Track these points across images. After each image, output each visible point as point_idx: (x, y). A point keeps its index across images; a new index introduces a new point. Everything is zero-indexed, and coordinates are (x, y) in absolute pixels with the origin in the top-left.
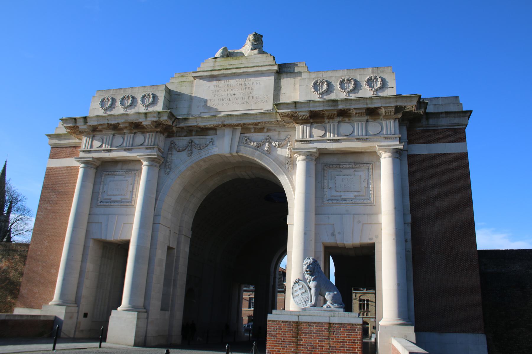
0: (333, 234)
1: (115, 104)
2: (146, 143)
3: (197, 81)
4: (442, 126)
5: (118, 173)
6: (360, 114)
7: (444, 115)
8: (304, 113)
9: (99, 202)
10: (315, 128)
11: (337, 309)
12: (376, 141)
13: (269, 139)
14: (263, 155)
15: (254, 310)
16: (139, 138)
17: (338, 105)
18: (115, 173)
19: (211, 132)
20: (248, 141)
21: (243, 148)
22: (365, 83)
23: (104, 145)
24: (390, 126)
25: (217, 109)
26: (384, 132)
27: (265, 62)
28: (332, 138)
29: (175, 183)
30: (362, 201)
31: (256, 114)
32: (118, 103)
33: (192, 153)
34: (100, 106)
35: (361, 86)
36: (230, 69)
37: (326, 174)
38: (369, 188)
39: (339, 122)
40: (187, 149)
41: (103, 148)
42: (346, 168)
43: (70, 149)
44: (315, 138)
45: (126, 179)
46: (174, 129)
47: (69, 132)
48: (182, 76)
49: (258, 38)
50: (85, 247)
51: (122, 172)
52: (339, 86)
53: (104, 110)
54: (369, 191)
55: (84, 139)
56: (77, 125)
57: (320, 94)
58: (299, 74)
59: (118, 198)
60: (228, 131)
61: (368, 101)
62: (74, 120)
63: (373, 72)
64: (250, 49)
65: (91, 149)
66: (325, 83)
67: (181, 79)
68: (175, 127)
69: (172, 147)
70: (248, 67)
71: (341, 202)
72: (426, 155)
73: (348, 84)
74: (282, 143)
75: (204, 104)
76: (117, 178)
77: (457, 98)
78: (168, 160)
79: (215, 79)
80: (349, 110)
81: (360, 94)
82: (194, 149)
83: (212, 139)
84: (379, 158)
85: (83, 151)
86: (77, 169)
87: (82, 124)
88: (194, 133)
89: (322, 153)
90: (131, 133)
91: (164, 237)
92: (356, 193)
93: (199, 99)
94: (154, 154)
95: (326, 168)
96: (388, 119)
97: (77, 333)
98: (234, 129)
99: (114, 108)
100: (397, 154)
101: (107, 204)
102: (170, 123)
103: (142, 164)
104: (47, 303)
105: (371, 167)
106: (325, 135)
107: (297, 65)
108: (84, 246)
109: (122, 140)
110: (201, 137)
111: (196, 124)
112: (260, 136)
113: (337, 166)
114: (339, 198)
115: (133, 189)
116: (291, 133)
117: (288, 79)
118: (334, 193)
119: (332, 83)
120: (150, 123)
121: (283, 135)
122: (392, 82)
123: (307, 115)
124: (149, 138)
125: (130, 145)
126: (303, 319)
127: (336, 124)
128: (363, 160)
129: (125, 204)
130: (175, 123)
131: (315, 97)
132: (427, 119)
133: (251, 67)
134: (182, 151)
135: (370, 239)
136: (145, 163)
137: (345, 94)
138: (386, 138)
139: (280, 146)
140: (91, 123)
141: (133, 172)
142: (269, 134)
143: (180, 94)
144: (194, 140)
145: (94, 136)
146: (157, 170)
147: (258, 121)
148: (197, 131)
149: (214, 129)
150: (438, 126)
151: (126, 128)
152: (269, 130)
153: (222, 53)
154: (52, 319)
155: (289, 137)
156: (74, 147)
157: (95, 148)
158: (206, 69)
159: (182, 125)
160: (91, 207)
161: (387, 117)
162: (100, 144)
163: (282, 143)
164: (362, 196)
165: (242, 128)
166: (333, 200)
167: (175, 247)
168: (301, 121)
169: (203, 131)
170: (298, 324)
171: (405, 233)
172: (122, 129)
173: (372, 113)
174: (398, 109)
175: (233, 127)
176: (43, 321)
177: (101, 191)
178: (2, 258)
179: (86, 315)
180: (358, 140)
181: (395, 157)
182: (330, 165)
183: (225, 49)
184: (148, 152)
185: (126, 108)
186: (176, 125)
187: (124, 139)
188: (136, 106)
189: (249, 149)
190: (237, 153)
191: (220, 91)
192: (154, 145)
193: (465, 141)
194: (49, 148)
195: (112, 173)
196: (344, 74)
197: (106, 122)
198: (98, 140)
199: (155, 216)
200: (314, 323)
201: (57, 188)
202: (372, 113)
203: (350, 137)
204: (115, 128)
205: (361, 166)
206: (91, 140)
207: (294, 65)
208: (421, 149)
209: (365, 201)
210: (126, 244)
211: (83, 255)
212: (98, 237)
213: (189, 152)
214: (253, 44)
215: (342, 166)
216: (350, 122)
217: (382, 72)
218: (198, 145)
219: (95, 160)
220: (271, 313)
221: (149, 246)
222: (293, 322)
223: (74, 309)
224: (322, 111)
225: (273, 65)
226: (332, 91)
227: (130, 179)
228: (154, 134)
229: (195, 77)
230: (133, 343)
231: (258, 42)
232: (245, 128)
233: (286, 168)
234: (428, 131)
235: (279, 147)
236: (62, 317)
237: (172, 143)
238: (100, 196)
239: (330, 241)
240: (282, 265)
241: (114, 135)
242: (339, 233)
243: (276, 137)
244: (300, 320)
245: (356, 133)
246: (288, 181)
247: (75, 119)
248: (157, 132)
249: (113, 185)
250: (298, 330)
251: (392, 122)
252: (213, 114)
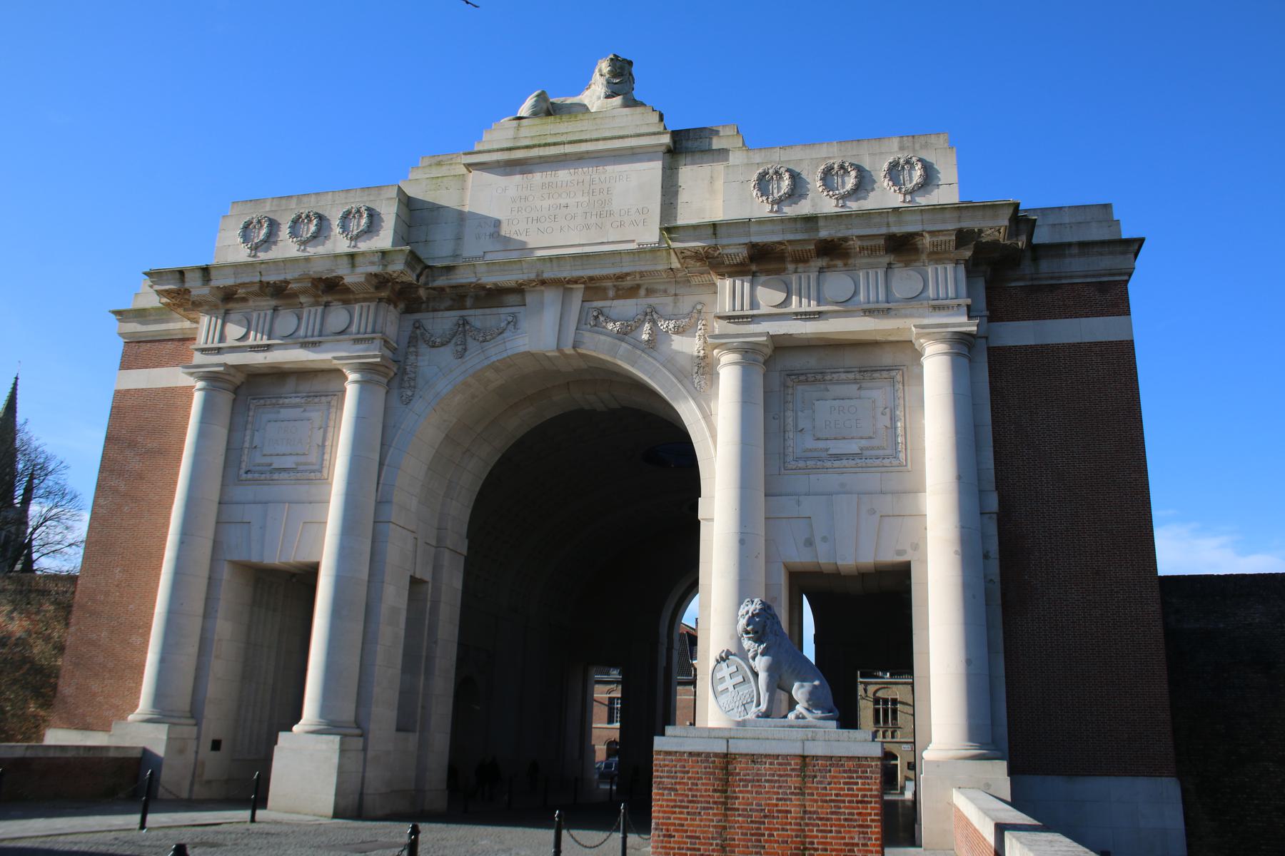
0: (809, 543)
1: (276, 235)
2: (354, 328)
3: (475, 173)
4: (1071, 277)
5: (287, 401)
6: (873, 251)
7: (1075, 251)
8: (734, 248)
9: (242, 471)
10: (764, 285)
11: (822, 723)
12: (911, 316)
13: (651, 315)
14: (639, 352)
15: (621, 728)
16: (338, 317)
17: (817, 230)
18: (281, 401)
19: (512, 298)
20: (602, 318)
21: (587, 337)
22: (883, 174)
23: (252, 333)
24: (946, 279)
25: (525, 243)
26: (931, 292)
27: (639, 125)
28: (805, 308)
29: (426, 423)
30: (878, 462)
31: (619, 253)
32: (284, 232)
33: (465, 350)
34: (240, 240)
35: (874, 182)
36: (555, 144)
37: (789, 398)
38: (896, 428)
39: (821, 270)
41: (250, 341)
42: (839, 382)
43: (170, 345)
44: (764, 309)
45: (307, 414)
46: (422, 292)
47: (167, 305)
48: (439, 164)
49: (622, 68)
50: (212, 582)
51: (298, 400)
52: (819, 183)
53: (251, 249)
54: (896, 436)
55: (205, 320)
56: (187, 285)
57: (773, 203)
58: (723, 153)
59: (289, 462)
60: (551, 297)
61: (892, 219)
62: (177, 275)
63: (902, 148)
64: (602, 95)
65: (221, 345)
66: (787, 176)
67: (436, 172)
68: (425, 288)
69: (417, 337)
70: (597, 140)
71: (828, 464)
72: (1031, 346)
73: (842, 176)
74: (684, 322)
75: (492, 230)
76: (285, 413)
77: (1107, 207)
79: (518, 168)
80: (845, 239)
81: (871, 202)
82: (469, 340)
83: (514, 315)
84: (918, 355)
85: (203, 350)
86: (187, 392)
87: (199, 283)
88: (469, 302)
89: (781, 346)
90: (317, 304)
91: (401, 555)
92: (864, 443)
93: (483, 220)
94: (373, 354)
95: (790, 383)
96: (938, 261)
97: (196, 787)
98: (566, 289)
99: (275, 243)
100: (963, 346)
101: (263, 476)
102: (411, 277)
103: (346, 378)
104: (125, 718)
105: (899, 378)
106: (786, 302)
107: (717, 132)
108: (210, 578)
109: (295, 321)
110: (488, 311)
111: (474, 280)
112: (628, 307)
113: (817, 378)
114: (824, 455)
115: (324, 440)
116: (705, 298)
117: (695, 167)
118: (810, 443)
119: (804, 175)
120: (362, 279)
121: (686, 303)
122: (948, 172)
123: (744, 253)
124: (361, 316)
125: (316, 333)
126: (738, 747)
127: (813, 276)
128: (881, 363)
129: (306, 475)
130: (423, 279)
131: (762, 209)
132: (1035, 260)
133: (605, 139)
134: (443, 345)
135: (899, 553)
136: (352, 376)
137: (834, 202)
138: (936, 308)
139: (679, 331)
140: (220, 281)
141: (324, 399)
142: (652, 301)
143: (436, 208)
145: (227, 312)
146: (381, 392)
147: (625, 270)
148: (477, 298)
149: (519, 289)
150: (1060, 278)
151: (304, 292)
152: (650, 292)
153: (535, 106)
154: (138, 754)
155: (699, 307)
156: (180, 340)
157: (230, 341)
158: (496, 146)
159: (441, 282)
160: (223, 485)
161: (937, 256)
162: (243, 331)
163: (684, 322)
164: (878, 448)
165: (587, 289)
166: (806, 459)
167: (427, 577)
168: (729, 270)
169: (492, 296)
170: (727, 758)
171: (984, 537)
172: (294, 295)
173: (901, 247)
174: (963, 237)
175: (564, 285)
176: (116, 759)
177: (247, 445)
178: (12, 612)
179: (216, 745)
180: (869, 312)
181: (958, 354)
182: (798, 375)
183: (542, 97)
184: (359, 350)
185: (304, 243)
186: (426, 283)
187: (299, 319)
188: (327, 238)
189: (603, 338)
190: (574, 348)
191: (531, 198)
192: (374, 332)
193: (1127, 312)
194: (120, 343)
196: (832, 153)
197: (257, 279)
198: (238, 323)
199: (379, 503)
200: (767, 756)
201: (140, 439)
202: (901, 247)
203: (847, 307)
204: (279, 292)
205: (876, 375)
206: (220, 322)
207: (710, 132)
208: (1020, 334)
209: (886, 462)
210: (311, 572)
211: (207, 599)
212: (242, 556)
213: (459, 348)
214: (608, 82)
215: (828, 377)
216: (848, 268)
217: (925, 146)
218: (479, 330)
219: (232, 371)
220: (663, 734)
221: (365, 576)
222: (716, 755)
223: (189, 731)
224: (780, 243)
225: (659, 133)
226: (803, 196)
227: (316, 416)
228: (373, 305)
229: (469, 166)
230: (331, 812)
231: (622, 79)
232: (593, 288)
233: (693, 383)
234: (1039, 289)
235: (677, 333)
236: (159, 750)
237: (417, 326)
238: (245, 458)
239: (801, 557)
240: (688, 619)
241: (275, 309)
242: (824, 539)
243: (670, 310)
244: (732, 750)
245: (862, 297)
246: (700, 416)
247: (181, 273)
248: (380, 300)
249: (276, 432)
250: (728, 774)
251: (950, 267)
252: (514, 256)
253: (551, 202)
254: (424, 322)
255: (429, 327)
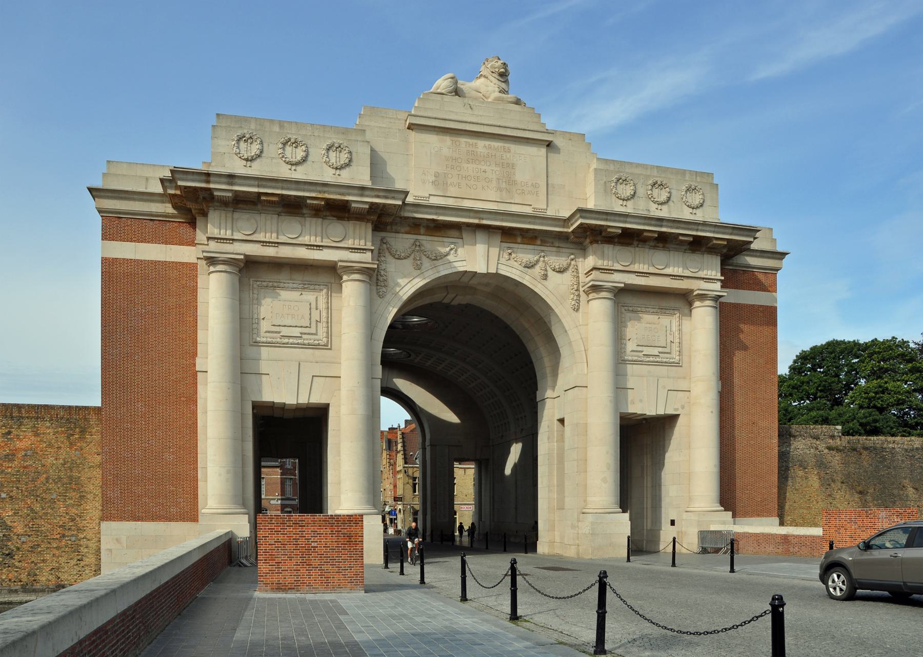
18: (282, 285)
19: (455, 233)
40: (412, 256)
51: (295, 286)
78: (382, 273)
110: (436, 239)
144: (424, 242)
195: (275, 284)
202: (698, 245)
237: (383, 241)
253: (475, 166)
254: (389, 239)
255: (393, 243)
